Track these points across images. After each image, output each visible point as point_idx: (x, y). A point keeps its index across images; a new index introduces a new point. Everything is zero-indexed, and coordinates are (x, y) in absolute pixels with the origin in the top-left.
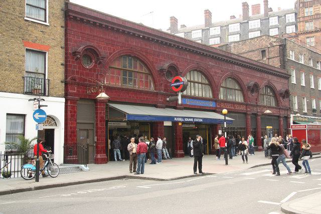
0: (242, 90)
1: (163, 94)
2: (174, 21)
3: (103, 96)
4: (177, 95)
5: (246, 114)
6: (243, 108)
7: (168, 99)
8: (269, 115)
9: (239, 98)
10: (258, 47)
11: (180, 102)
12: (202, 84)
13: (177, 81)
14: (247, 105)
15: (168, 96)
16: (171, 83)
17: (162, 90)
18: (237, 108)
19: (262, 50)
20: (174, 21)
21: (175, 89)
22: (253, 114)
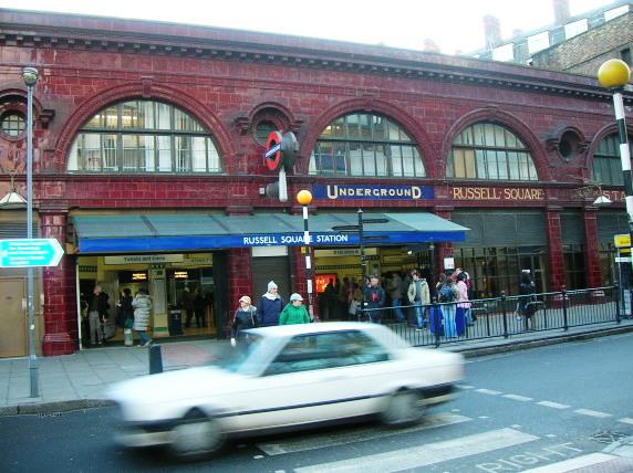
0: (529, 149)
1: (242, 180)
2: (492, 26)
3: (11, 200)
4: (278, 179)
5: (543, 209)
6: (534, 195)
7: (262, 191)
8: (603, 208)
9: (528, 172)
10: (614, 44)
11: (283, 195)
12: (506, 150)
13: (273, 143)
14: (543, 187)
15: (264, 183)
16: (264, 150)
17: (242, 170)
18: (510, 195)
19: (622, 48)
20: (492, 26)
21: (272, 165)
22: (566, 209)
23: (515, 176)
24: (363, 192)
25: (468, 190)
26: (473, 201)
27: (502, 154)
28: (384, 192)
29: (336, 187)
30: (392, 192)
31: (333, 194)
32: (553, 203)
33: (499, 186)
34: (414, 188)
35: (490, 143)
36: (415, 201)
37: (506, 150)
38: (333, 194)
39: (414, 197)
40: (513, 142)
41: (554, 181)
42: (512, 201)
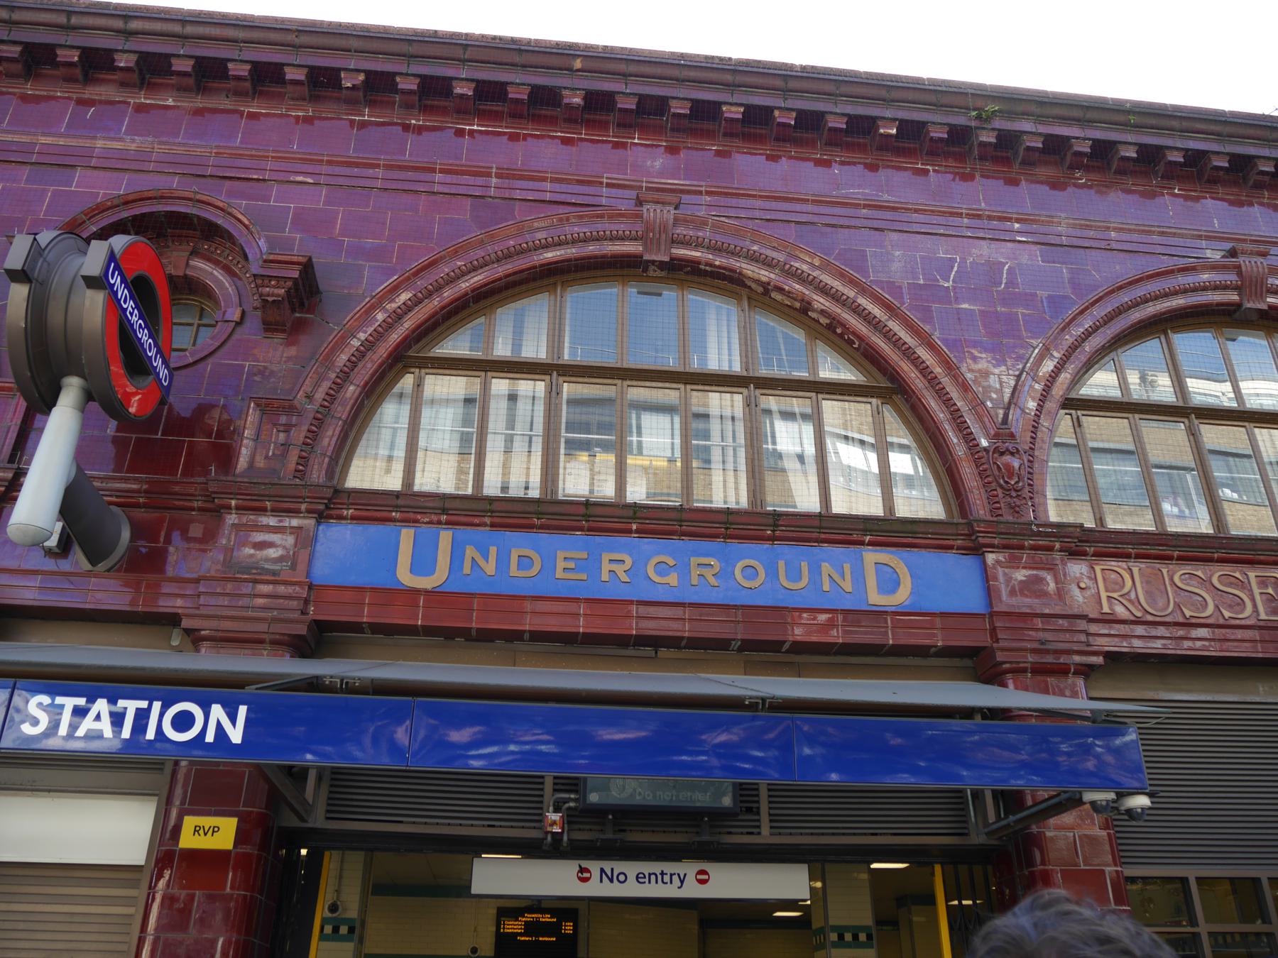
24: (592, 564)
34: (872, 557)
38: (421, 564)
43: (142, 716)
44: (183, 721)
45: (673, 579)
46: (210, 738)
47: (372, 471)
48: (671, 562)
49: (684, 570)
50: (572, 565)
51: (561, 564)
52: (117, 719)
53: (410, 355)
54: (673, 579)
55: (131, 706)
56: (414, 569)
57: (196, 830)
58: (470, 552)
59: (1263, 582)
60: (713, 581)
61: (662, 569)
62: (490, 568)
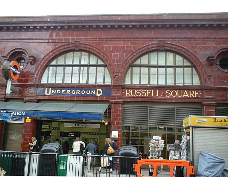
18: (170, 94)
23: (180, 82)
24: (66, 92)
25: (136, 91)
26: (141, 97)
27: (170, 70)
28: (78, 92)
29: (50, 89)
30: (83, 92)
31: (48, 92)
32: (208, 99)
33: (162, 88)
34: (98, 90)
35: (162, 62)
36: (98, 96)
37: (175, 67)
38: (48, 92)
39: (97, 95)
40: (179, 60)
41: (210, 85)
42: (171, 98)
43: (17, 113)
44: (20, 113)
45: (74, 93)
46: (22, 115)
47: (44, 81)
48: (74, 91)
49: (76, 92)
50: (64, 92)
51: (62, 92)
52: (15, 113)
53: (47, 66)
54: (74, 93)
55: (16, 112)
56: (47, 93)
57: (27, 120)
58: (53, 91)
59: (148, 91)
60: (79, 93)
61: (73, 92)
62: (55, 93)
